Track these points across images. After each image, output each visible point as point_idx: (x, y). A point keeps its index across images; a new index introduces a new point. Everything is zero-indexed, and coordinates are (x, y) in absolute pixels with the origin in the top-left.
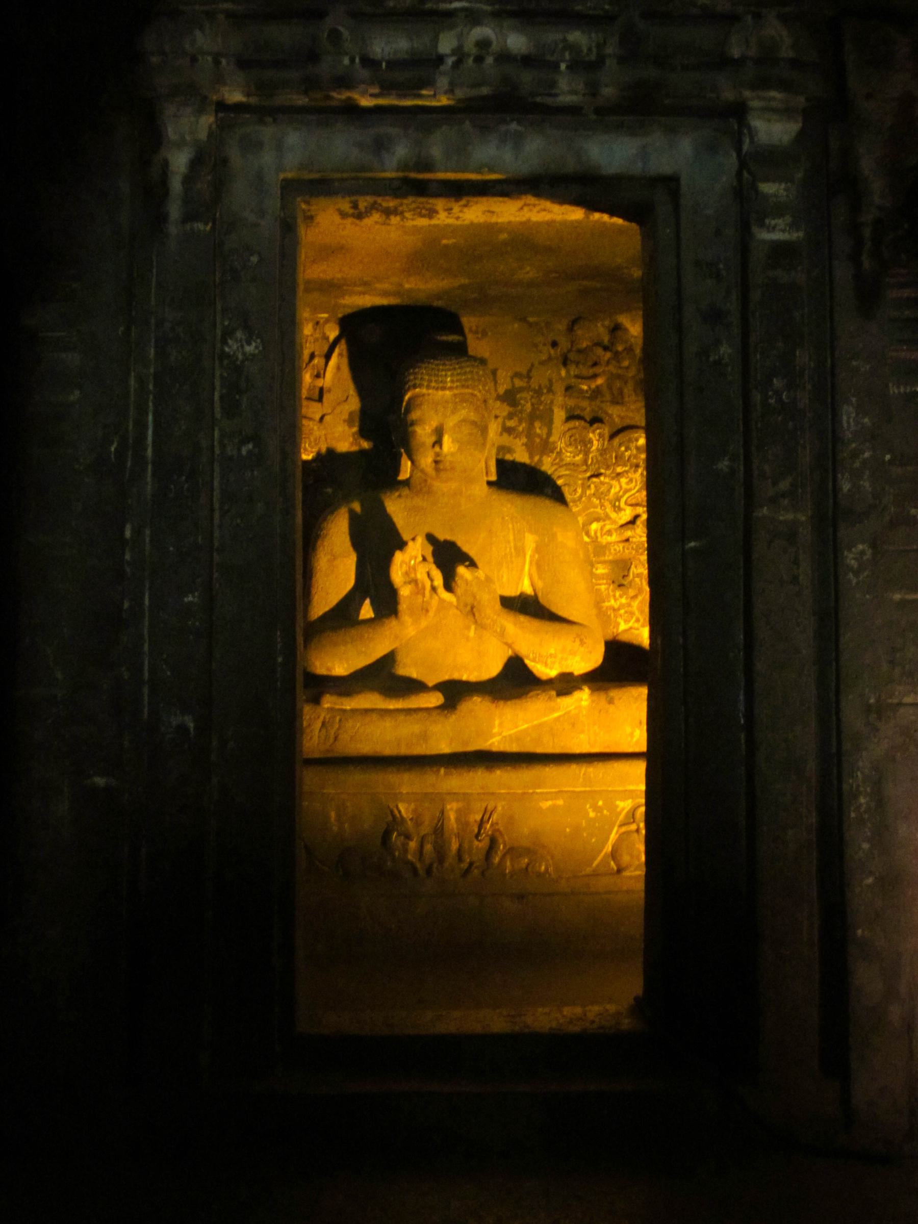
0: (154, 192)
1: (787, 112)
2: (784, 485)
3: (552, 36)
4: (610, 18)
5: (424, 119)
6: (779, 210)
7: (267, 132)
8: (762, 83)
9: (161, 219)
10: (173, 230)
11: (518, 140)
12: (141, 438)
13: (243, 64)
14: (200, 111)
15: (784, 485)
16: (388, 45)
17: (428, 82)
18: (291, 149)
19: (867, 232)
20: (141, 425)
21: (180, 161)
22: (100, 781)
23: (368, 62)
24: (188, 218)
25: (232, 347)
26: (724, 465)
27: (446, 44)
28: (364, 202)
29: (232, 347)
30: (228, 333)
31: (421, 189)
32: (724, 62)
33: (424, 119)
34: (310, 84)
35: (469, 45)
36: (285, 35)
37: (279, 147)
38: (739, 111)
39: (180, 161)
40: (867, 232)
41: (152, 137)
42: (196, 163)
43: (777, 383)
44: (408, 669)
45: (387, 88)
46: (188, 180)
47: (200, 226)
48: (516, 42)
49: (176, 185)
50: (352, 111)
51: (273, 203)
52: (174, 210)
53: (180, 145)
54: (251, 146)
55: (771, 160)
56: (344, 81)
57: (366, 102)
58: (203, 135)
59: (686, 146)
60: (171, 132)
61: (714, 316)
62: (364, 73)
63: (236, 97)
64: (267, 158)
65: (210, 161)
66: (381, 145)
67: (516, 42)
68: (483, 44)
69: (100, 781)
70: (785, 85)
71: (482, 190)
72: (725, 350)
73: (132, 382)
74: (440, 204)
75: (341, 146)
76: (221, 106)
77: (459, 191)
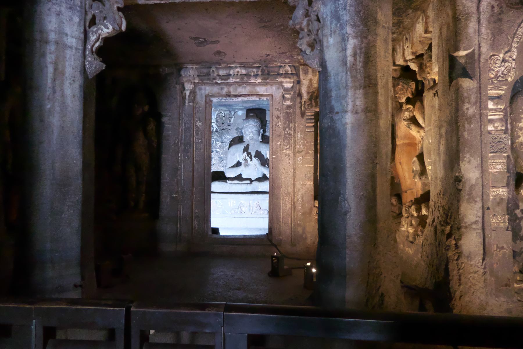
0: (184, 98)
1: (290, 82)
2: (288, 147)
3: (250, 70)
4: (260, 67)
5: (229, 85)
6: (288, 99)
7: (203, 87)
8: (285, 77)
9: (184, 103)
10: (187, 104)
11: (245, 87)
12: (181, 139)
13: (198, 76)
14: (191, 84)
15: (288, 147)
16: (222, 72)
17: (229, 79)
18: (207, 89)
19: (303, 103)
20: (182, 137)
21: (188, 93)
22: (174, 195)
23: (219, 75)
24: (189, 102)
25: (197, 124)
26: (279, 143)
27: (231, 72)
28: (220, 98)
29: (197, 124)
30: (197, 121)
31: (229, 96)
32: (279, 75)
33: (229, 85)
34: (209, 79)
35: (236, 73)
36: (205, 71)
37: (205, 89)
38: (282, 82)
39: (188, 93)
40: (303, 103)
41: (184, 89)
42: (190, 93)
43: (287, 129)
44: (244, 176)
45: (222, 80)
46: (189, 96)
47: (191, 104)
48: (244, 72)
49: (187, 97)
50: (216, 83)
51: (204, 99)
52: (187, 102)
53: (187, 90)
54: (200, 89)
55: (286, 90)
56: (214, 79)
57: (219, 82)
58: (191, 88)
59: (274, 88)
60: (186, 88)
61: (278, 118)
62: (218, 78)
63: (197, 81)
64: (203, 91)
65: (193, 92)
66: (222, 89)
67: (244, 72)
68: (238, 72)
69: (174, 195)
70: (289, 78)
71: (240, 96)
72: (280, 123)
73: (180, 130)
74: (233, 98)
75: (215, 89)
76: (195, 83)
77: (236, 96)
